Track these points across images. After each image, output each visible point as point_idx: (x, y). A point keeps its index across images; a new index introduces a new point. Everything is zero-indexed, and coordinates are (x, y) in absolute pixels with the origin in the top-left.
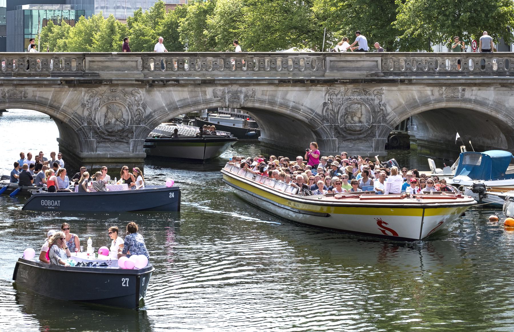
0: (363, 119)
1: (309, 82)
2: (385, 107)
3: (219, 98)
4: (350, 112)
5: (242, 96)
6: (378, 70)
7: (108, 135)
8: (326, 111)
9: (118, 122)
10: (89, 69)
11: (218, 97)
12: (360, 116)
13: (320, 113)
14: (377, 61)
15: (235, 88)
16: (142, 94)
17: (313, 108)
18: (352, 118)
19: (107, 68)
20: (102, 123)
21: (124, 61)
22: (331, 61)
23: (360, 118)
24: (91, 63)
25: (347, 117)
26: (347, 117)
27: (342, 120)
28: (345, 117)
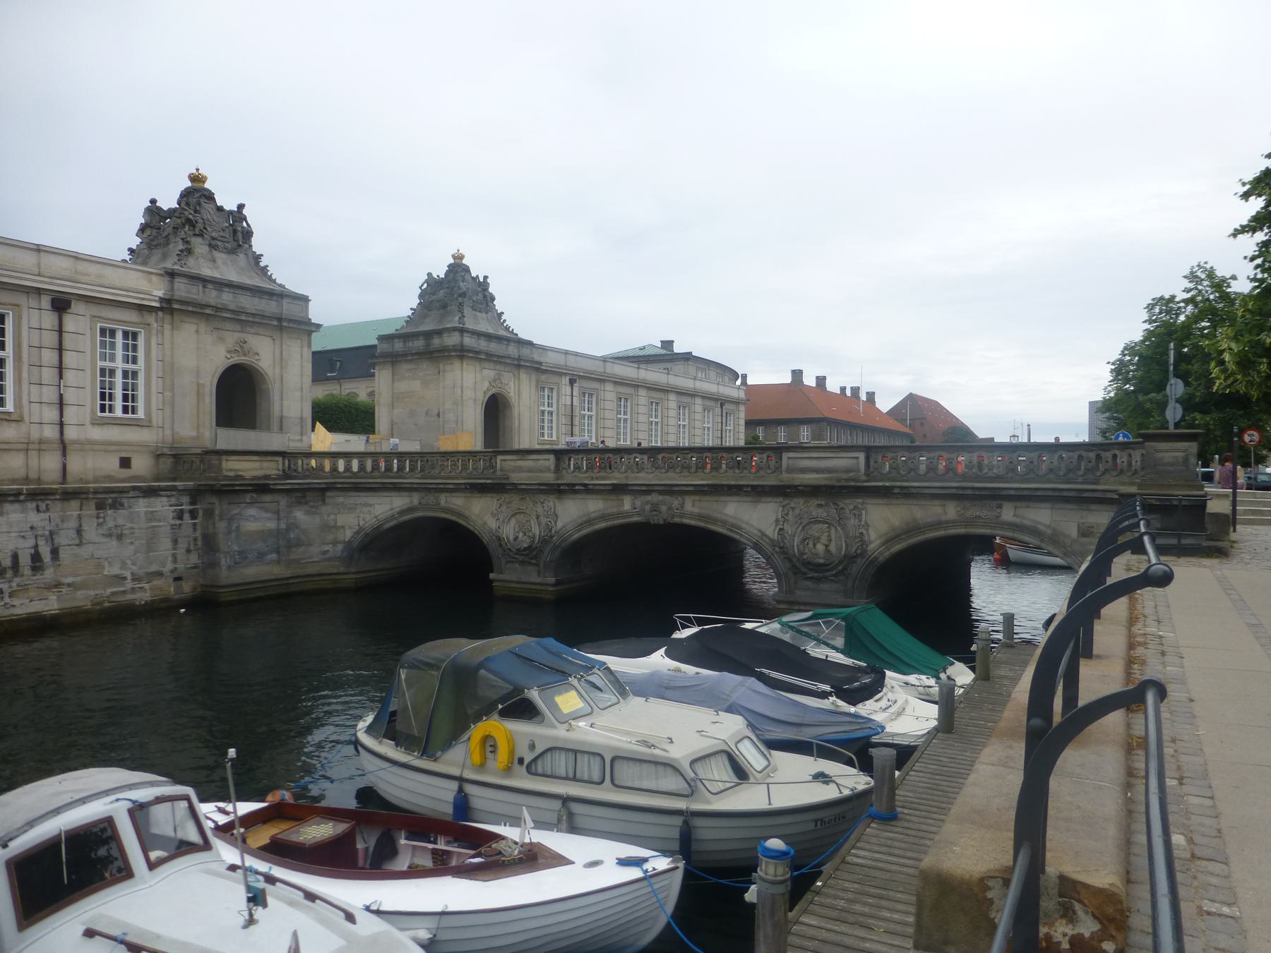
0: (833, 548)
1: (749, 489)
2: (867, 530)
3: (638, 510)
4: (810, 535)
5: (664, 508)
6: (858, 470)
7: (516, 554)
8: (778, 534)
9: (525, 537)
10: (501, 470)
11: (635, 508)
12: (827, 543)
13: (771, 536)
14: (857, 458)
15: (655, 498)
16: (551, 502)
17: (763, 530)
18: (815, 545)
19: (520, 469)
20: (511, 538)
21: (537, 460)
22: (789, 458)
23: (827, 546)
24: (503, 462)
25: (808, 543)
26: (808, 543)
27: (801, 547)
28: (806, 543)
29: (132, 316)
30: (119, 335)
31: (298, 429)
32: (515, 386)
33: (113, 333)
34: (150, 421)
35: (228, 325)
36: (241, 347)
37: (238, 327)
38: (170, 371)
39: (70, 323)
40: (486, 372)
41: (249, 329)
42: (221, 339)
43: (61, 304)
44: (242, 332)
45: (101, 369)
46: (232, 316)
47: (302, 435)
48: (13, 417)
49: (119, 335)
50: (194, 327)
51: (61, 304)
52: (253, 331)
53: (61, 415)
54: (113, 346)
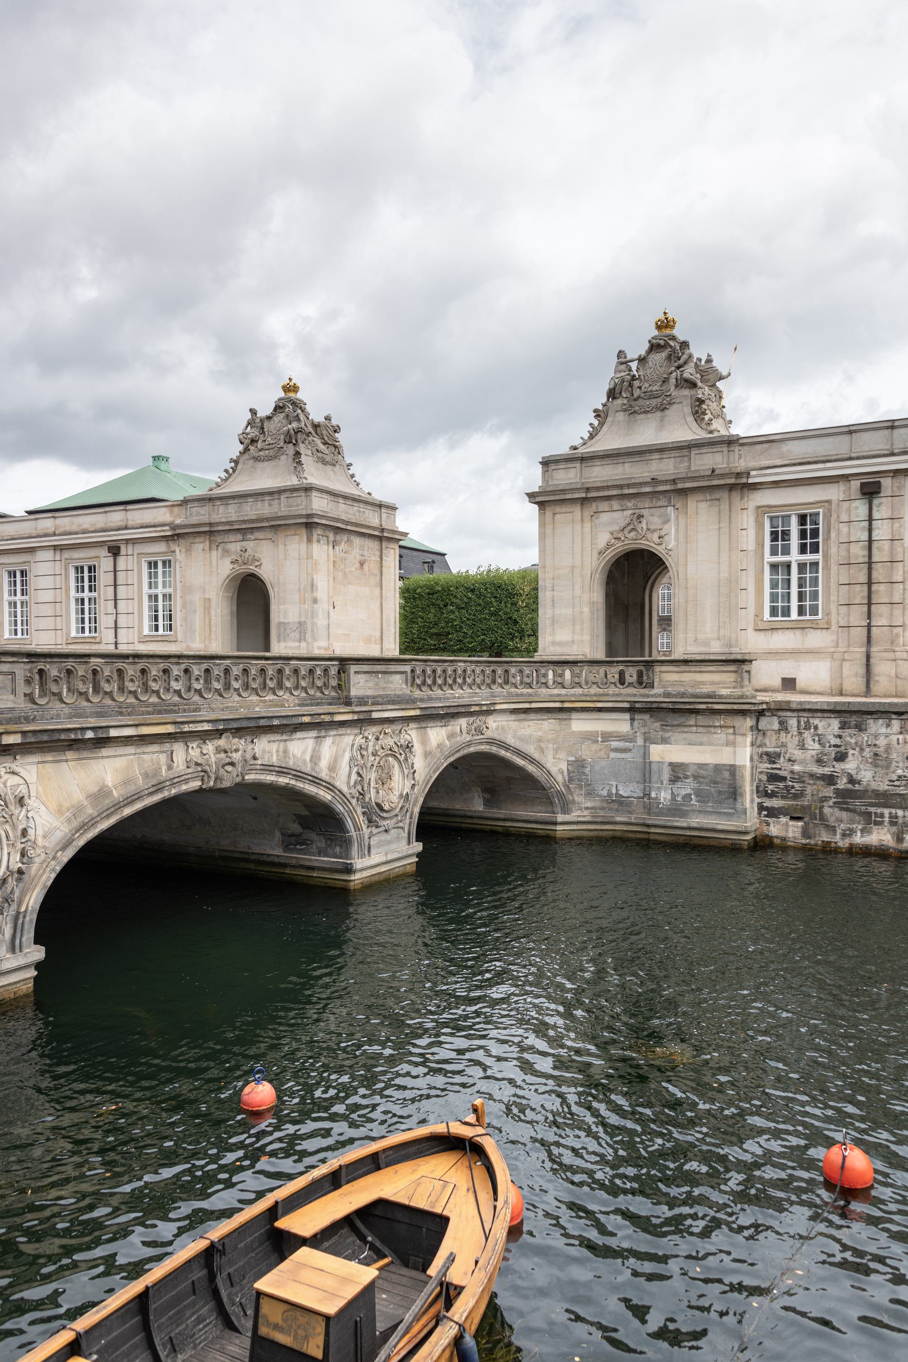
29: (161, 547)
30: (160, 565)
31: (296, 635)
32: (677, 530)
33: (156, 563)
34: (176, 636)
35: (232, 537)
36: (241, 556)
37: (240, 537)
38: (188, 589)
39: (122, 562)
40: (605, 517)
41: (249, 536)
42: (226, 552)
43: (115, 551)
44: (243, 540)
45: (818, 552)
46: (227, 528)
47: (300, 641)
48: (98, 640)
49: (160, 565)
50: (201, 546)
51: (115, 551)
52: (253, 537)
53: (116, 637)
54: (156, 576)
